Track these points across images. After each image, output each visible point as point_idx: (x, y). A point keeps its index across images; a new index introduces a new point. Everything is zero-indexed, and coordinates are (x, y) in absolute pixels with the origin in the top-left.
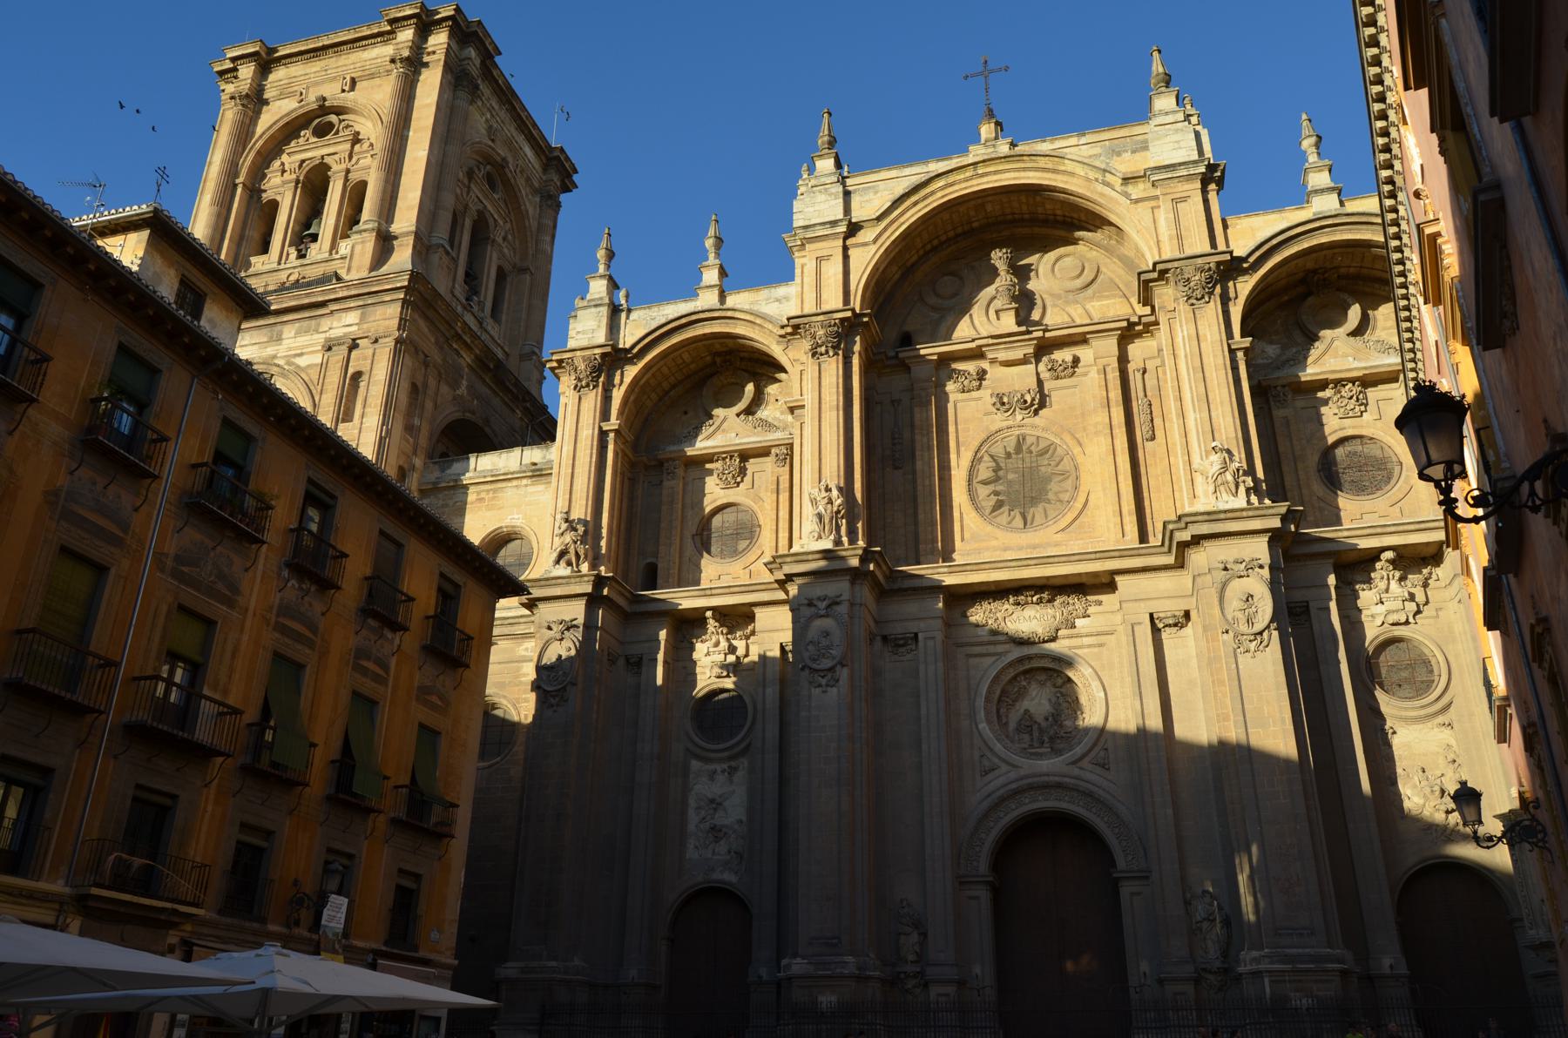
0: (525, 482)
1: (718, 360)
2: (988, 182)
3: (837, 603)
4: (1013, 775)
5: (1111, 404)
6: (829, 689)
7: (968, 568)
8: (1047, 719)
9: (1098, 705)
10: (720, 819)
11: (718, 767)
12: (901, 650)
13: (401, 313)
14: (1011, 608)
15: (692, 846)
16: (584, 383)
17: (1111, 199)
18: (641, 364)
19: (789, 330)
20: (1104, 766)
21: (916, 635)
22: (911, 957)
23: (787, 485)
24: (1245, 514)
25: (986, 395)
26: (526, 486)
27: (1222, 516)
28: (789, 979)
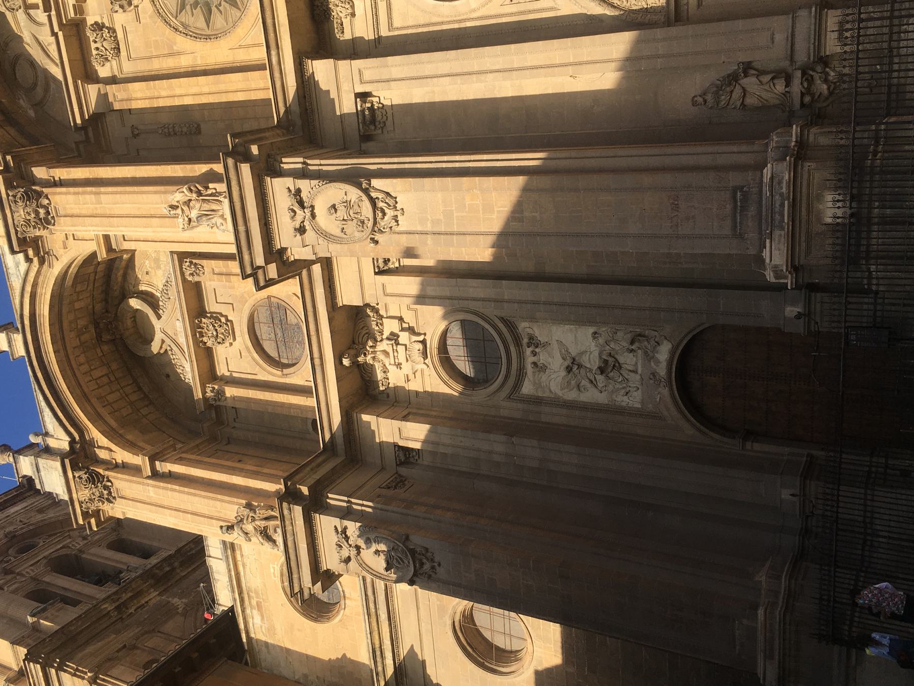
0: (239, 557)
1: (106, 337)
3: (298, 191)
6: (399, 206)
10: (592, 361)
11: (530, 359)
13: (70, 673)
15: (625, 398)
16: (105, 492)
18: (90, 425)
19: (31, 252)
22: (780, 86)
23: (221, 263)
25: (121, 19)
26: (242, 556)
28: (795, 268)
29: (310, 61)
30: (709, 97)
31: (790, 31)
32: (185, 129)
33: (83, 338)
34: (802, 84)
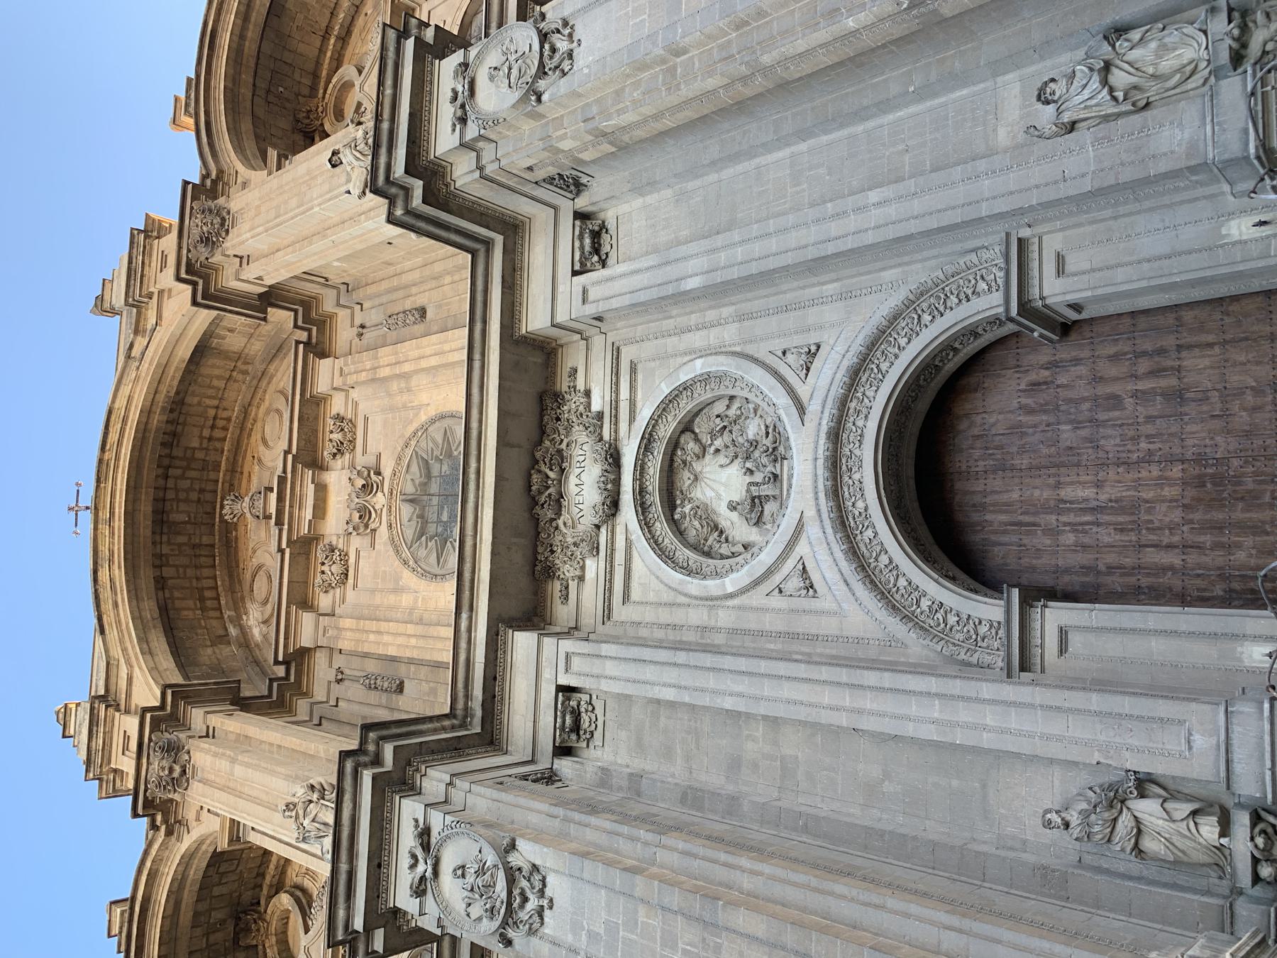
2: (120, 508)
4: (813, 530)
5: (376, 365)
6: (548, 892)
7: (467, 575)
8: (751, 472)
9: (713, 369)
12: (585, 718)
14: (565, 516)
17: (155, 352)
19: (159, 818)
20: (812, 355)
21: (561, 689)
24: (389, 91)
27: (385, 126)
29: (511, 631)
30: (1074, 819)
31: (1223, 737)
32: (386, 685)
33: (212, 938)
34: (1252, 839)
